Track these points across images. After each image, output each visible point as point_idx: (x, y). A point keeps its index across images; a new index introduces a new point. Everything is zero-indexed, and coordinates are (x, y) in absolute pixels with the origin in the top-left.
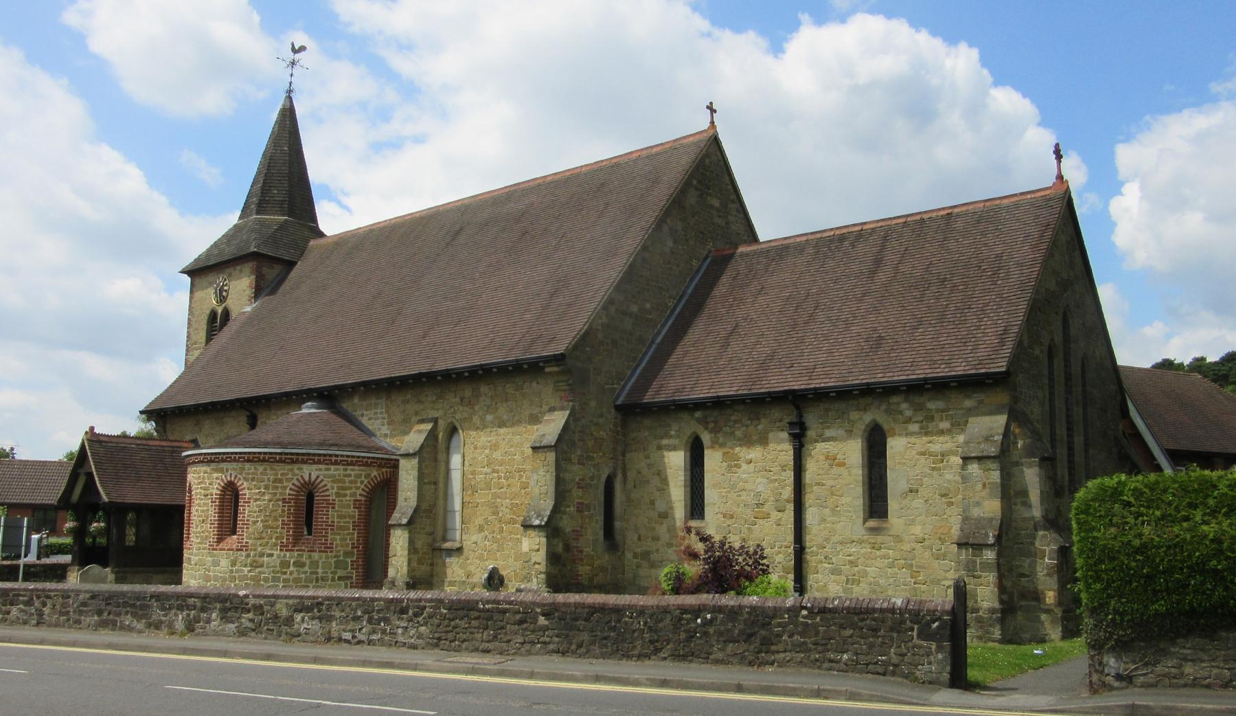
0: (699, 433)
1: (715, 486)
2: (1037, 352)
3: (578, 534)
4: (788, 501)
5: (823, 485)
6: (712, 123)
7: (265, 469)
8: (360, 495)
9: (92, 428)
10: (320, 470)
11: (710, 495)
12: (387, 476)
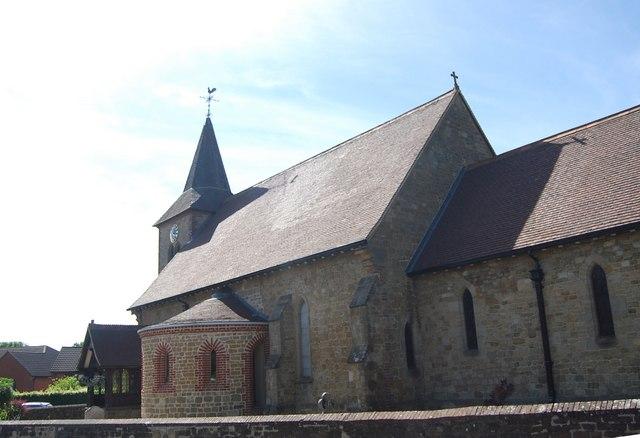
4: (537, 329)
5: (561, 314)
6: (456, 84)
9: (93, 321)
11: (480, 330)
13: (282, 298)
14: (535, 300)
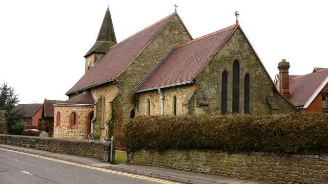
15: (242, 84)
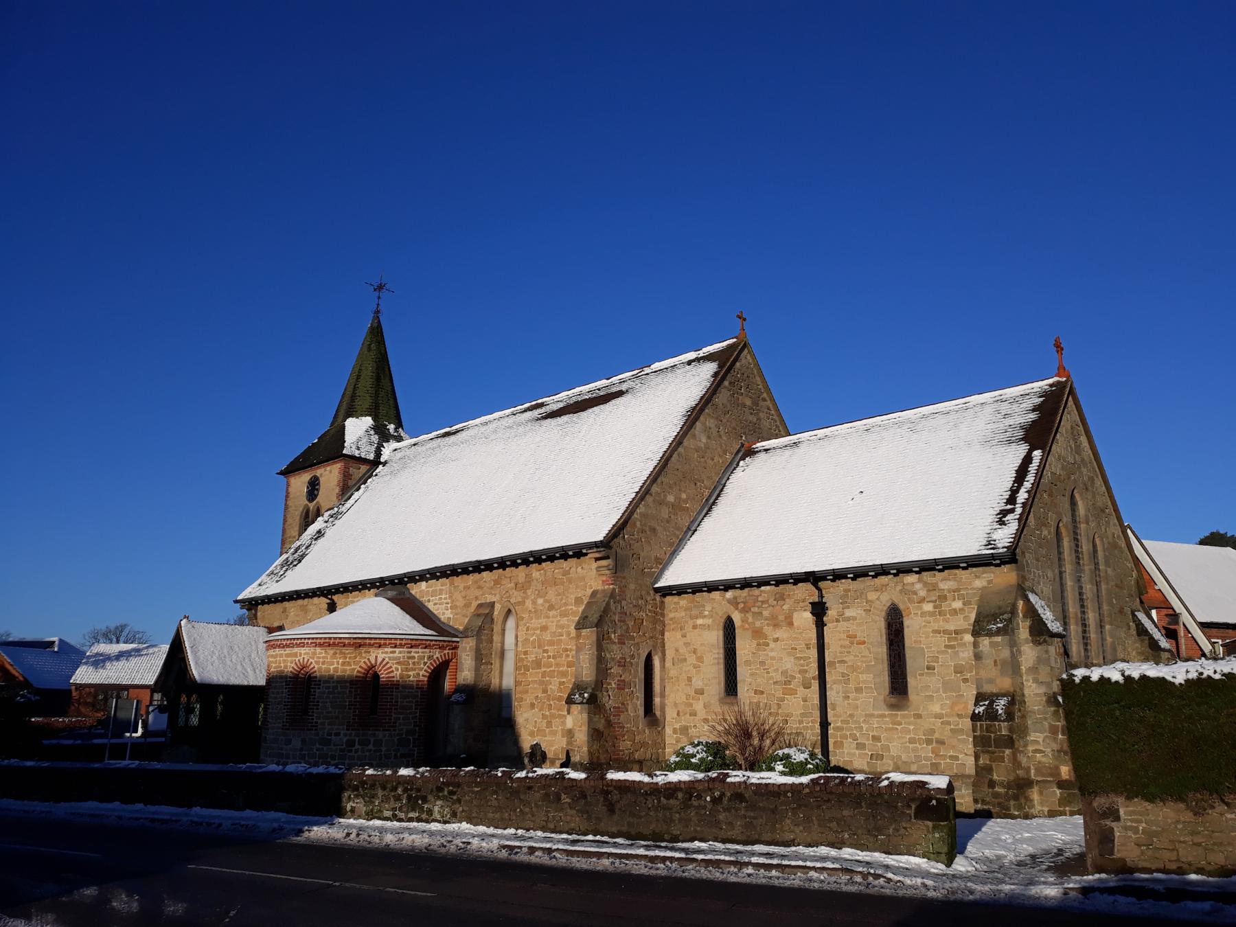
0: (730, 613)
1: (748, 663)
2: (1045, 532)
3: (619, 711)
7: (335, 653)
8: (423, 676)
10: (386, 653)
11: (742, 671)
12: (449, 656)
13: (480, 606)
14: (814, 641)
15: (1087, 568)
